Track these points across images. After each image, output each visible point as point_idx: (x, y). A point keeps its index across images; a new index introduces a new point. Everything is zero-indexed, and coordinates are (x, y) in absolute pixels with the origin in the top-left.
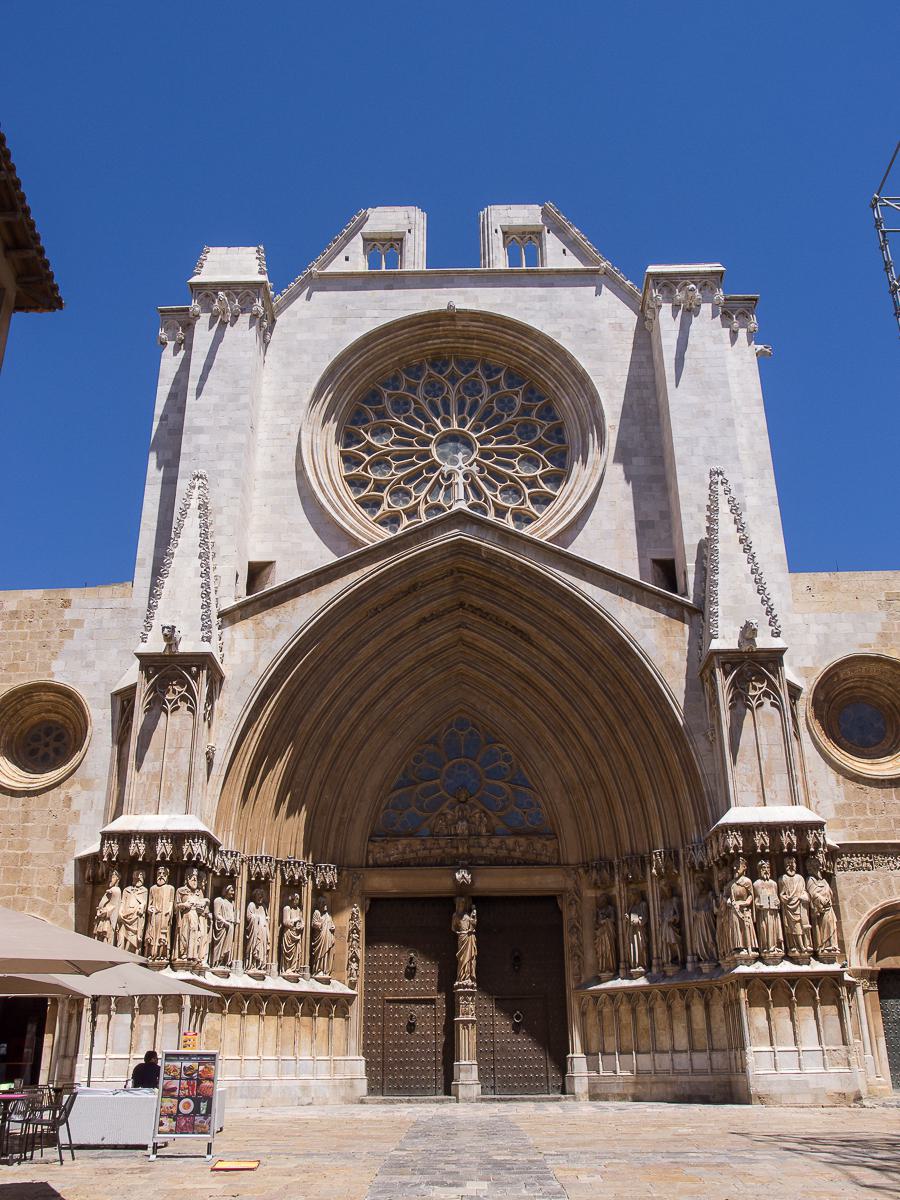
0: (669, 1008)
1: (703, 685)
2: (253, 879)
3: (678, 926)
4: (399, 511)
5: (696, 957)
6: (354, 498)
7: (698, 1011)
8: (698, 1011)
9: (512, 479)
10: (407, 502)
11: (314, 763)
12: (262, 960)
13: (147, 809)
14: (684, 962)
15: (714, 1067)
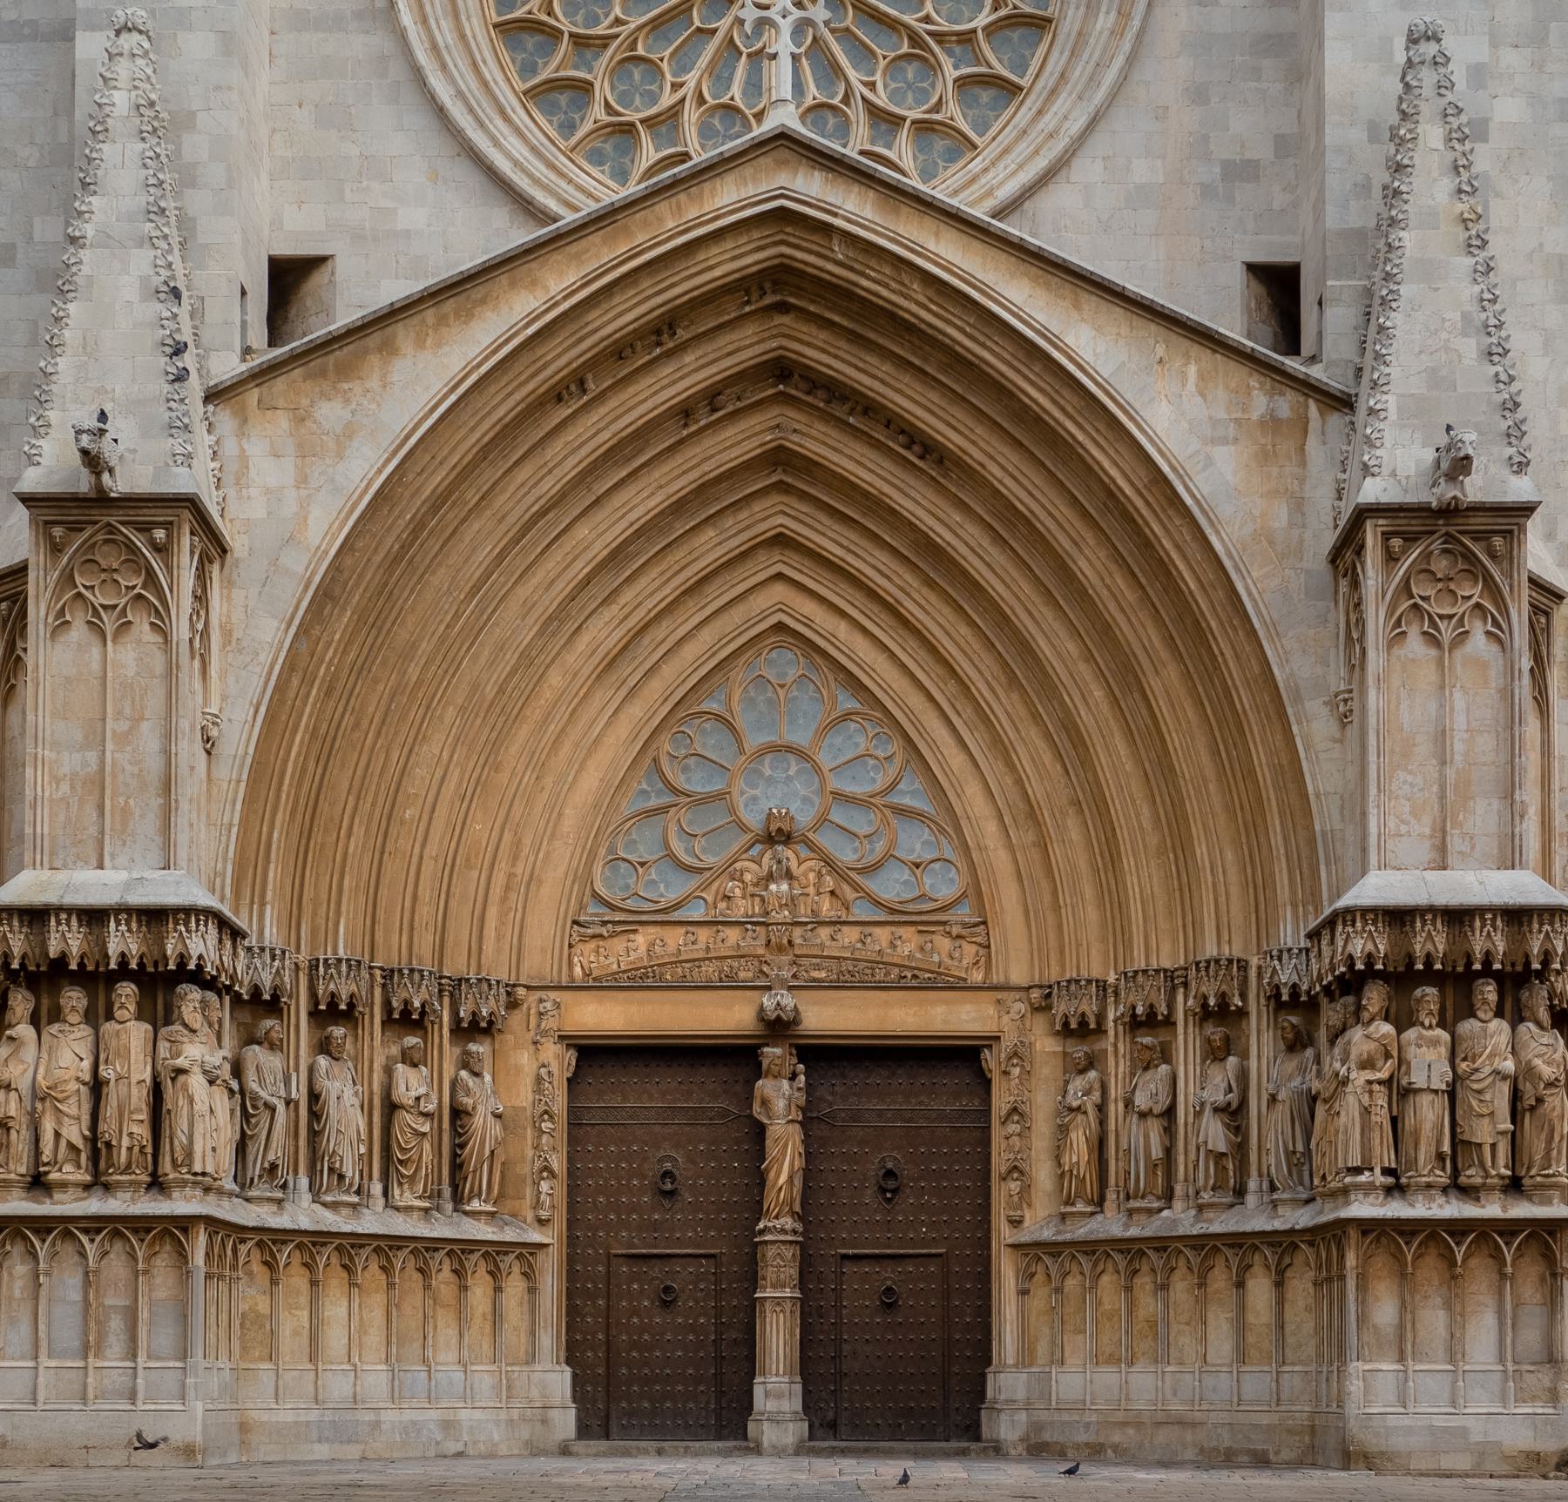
0: (1202, 1284)
1: (1337, 585)
2: (322, 1007)
3: (1234, 1114)
4: (632, 125)
5: (1265, 1185)
6: (521, 86)
7: (1260, 1288)
8: (1260, 1288)
9: (915, 39)
10: (653, 99)
11: (445, 755)
12: (349, 1174)
13: (78, 857)
14: (1240, 1192)
15: (1284, 1396)
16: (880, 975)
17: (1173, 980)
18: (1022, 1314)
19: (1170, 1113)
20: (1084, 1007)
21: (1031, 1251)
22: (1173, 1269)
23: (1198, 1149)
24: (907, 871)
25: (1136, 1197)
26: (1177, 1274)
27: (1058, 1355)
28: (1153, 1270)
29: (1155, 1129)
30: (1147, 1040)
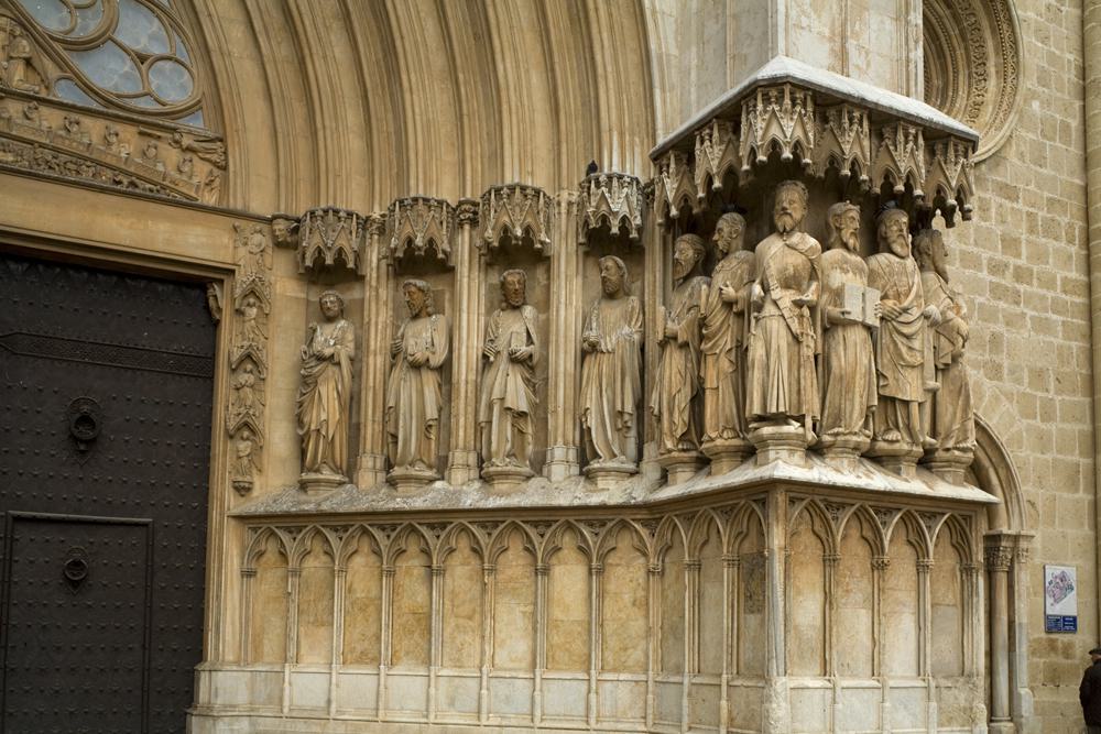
7: (569, 577)
8: (569, 577)
16: (87, 175)
17: (466, 215)
18: (245, 600)
19: (445, 370)
20: (342, 242)
21: (261, 524)
22: (452, 551)
23: (490, 407)
24: (129, 63)
25: (401, 465)
26: (457, 558)
27: (292, 652)
28: (426, 552)
29: (430, 381)
30: (420, 283)
